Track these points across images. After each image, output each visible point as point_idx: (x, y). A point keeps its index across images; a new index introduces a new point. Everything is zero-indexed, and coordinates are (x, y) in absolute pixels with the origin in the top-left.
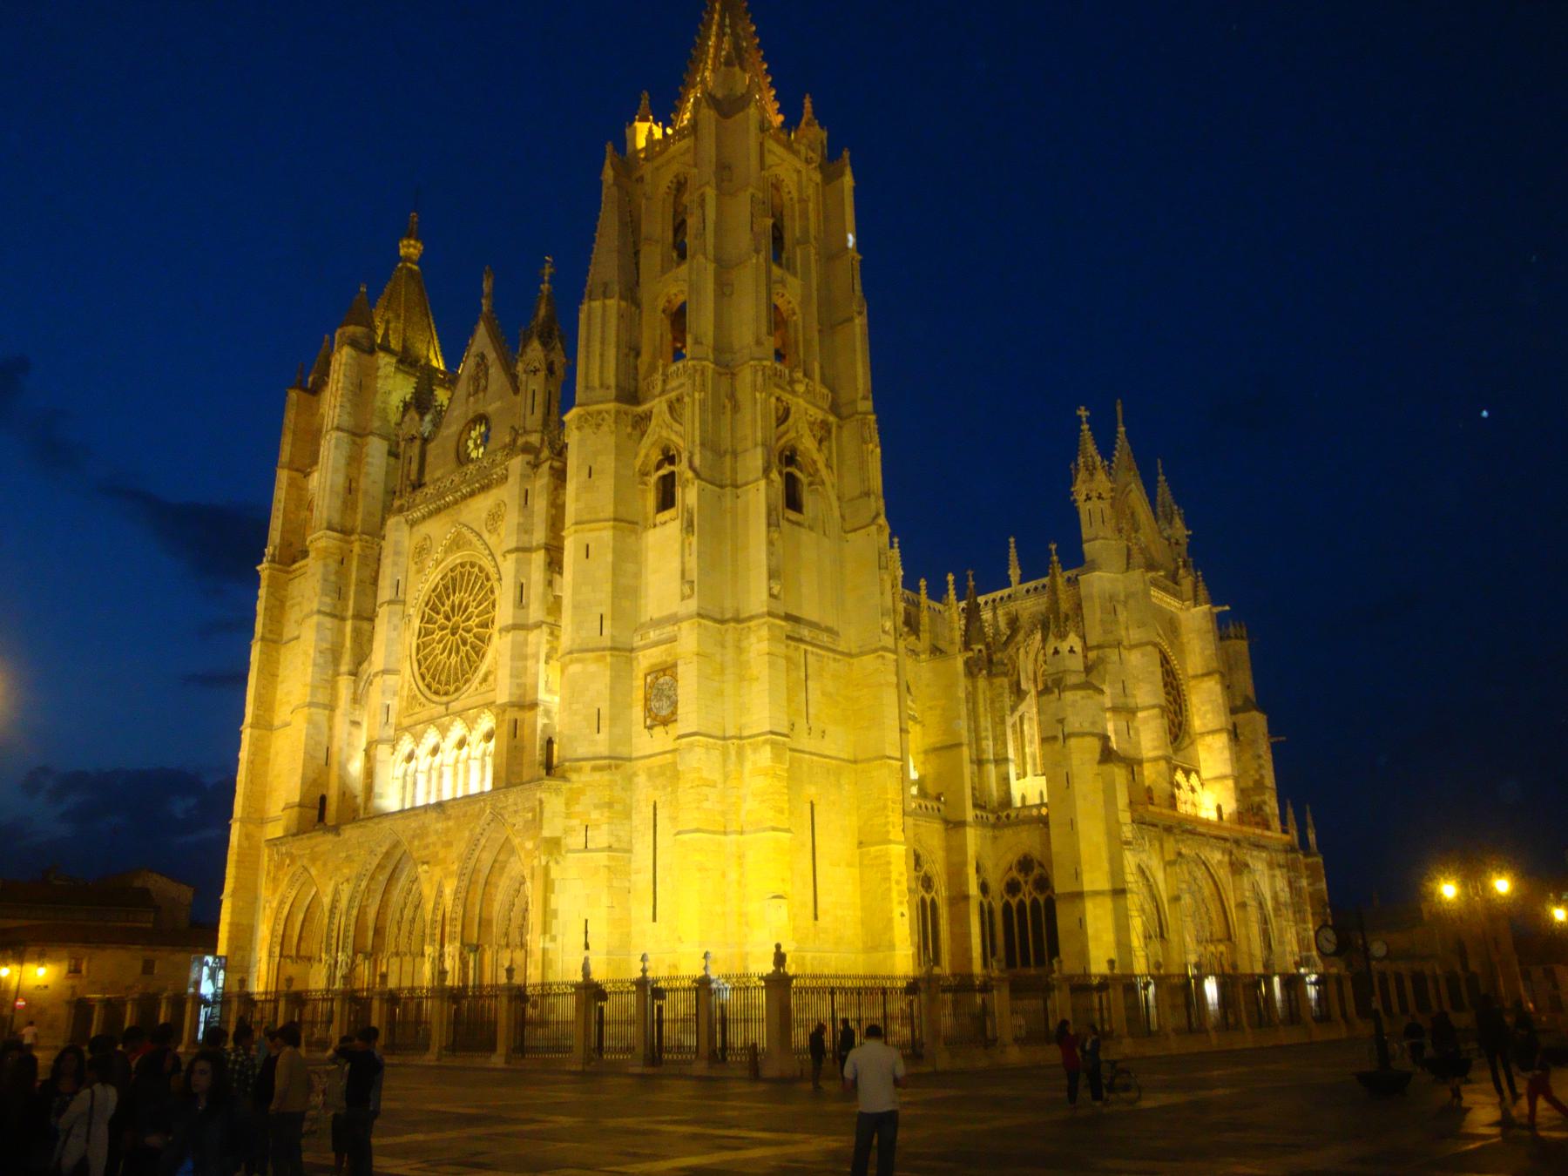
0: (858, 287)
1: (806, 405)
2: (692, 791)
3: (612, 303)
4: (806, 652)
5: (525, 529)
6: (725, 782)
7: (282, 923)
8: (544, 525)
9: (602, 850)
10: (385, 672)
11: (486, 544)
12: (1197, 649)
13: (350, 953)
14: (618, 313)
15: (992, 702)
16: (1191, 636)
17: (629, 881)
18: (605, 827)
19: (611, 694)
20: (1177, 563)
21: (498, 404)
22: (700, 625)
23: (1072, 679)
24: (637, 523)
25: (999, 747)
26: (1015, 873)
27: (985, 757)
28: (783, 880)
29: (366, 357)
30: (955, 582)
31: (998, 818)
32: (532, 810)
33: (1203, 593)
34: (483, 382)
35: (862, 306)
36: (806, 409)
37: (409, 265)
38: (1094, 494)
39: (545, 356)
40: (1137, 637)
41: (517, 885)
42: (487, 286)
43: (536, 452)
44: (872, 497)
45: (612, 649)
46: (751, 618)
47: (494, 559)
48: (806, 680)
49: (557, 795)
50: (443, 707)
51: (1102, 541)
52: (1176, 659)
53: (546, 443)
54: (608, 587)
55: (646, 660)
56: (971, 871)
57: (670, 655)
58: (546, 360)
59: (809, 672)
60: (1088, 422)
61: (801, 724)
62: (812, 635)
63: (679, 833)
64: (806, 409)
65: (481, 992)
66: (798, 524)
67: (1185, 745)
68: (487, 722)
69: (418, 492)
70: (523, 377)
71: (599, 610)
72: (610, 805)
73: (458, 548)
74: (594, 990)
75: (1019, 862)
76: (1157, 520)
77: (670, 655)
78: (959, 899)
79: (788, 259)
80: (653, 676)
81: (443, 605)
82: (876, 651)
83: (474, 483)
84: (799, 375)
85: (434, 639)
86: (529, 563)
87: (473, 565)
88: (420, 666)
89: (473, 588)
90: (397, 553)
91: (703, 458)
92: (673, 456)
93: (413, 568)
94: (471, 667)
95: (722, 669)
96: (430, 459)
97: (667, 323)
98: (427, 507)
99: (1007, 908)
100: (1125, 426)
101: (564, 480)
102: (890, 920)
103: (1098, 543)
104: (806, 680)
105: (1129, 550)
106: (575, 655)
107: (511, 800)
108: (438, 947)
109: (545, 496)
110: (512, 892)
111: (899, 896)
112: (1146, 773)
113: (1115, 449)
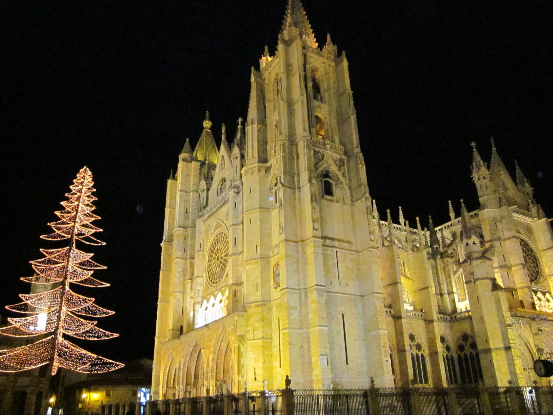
0: (352, 103)
1: (332, 153)
3: (255, 126)
4: (336, 252)
6: (301, 307)
10: (197, 277)
12: (543, 238)
13: (185, 385)
14: (257, 129)
15: (444, 269)
17: (272, 351)
18: (261, 329)
20: (528, 202)
21: (228, 172)
22: (286, 244)
23: (475, 255)
25: (449, 288)
26: (461, 342)
29: (189, 164)
30: (420, 220)
31: (452, 318)
33: (542, 213)
35: (354, 111)
37: (207, 130)
38: (481, 177)
42: (223, 130)
44: (363, 186)
45: (261, 258)
46: (307, 239)
51: (487, 196)
52: (534, 245)
55: (273, 262)
64: (332, 155)
66: (332, 201)
67: (541, 281)
69: (205, 209)
72: (262, 320)
75: (462, 336)
76: (516, 185)
80: (276, 267)
81: (214, 249)
82: (368, 249)
90: (200, 233)
91: (285, 178)
100: (496, 147)
103: (485, 197)
105: (500, 198)
106: (248, 262)
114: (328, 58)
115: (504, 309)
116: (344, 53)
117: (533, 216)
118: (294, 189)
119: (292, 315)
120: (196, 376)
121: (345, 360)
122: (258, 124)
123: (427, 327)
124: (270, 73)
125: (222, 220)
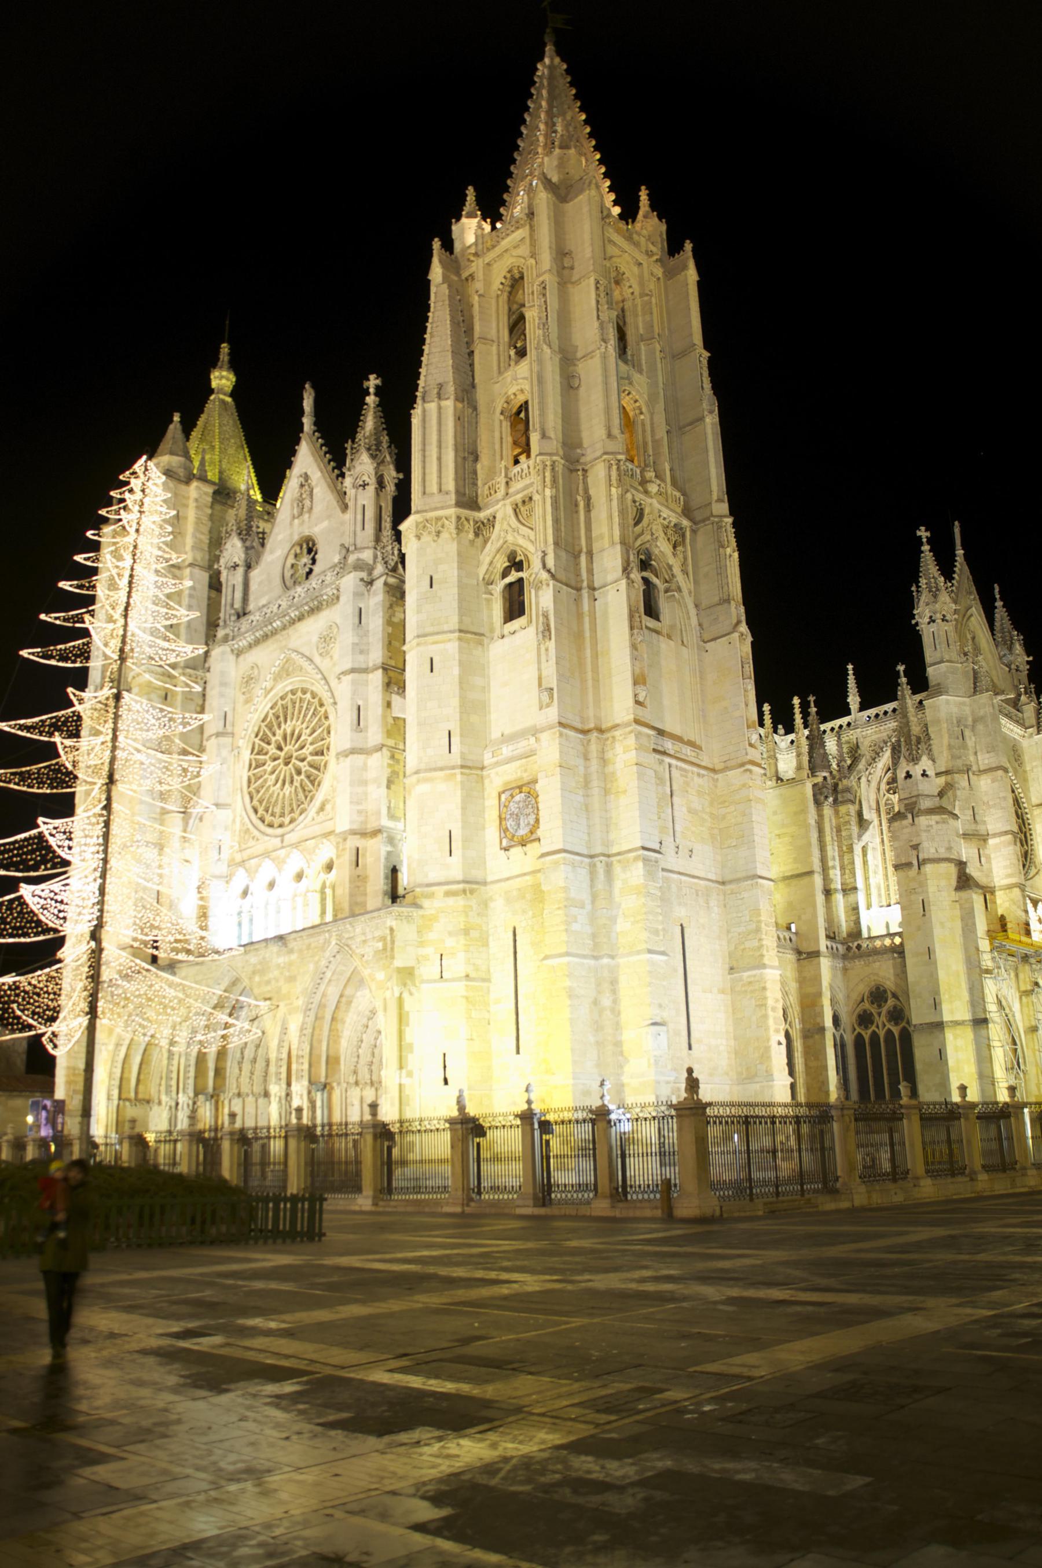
0: (707, 385)
1: (660, 507)
2: (560, 912)
3: (449, 404)
4: (670, 766)
5: (361, 649)
6: (593, 902)
7: (120, 1066)
8: (380, 645)
9: (459, 979)
11: (317, 667)
13: (192, 1094)
15: (839, 831)
16: (1034, 764)
19: (464, 814)
21: (325, 524)
22: (561, 735)
23: (925, 804)
24: (483, 635)
25: (847, 877)
26: (866, 1005)
27: (833, 886)
28: (660, 1006)
29: (183, 487)
31: (849, 949)
32: (383, 939)
34: (307, 503)
36: (660, 511)
37: (222, 396)
38: (939, 616)
39: (377, 469)
40: (986, 762)
41: (365, 1021)
42: (308, 403)
43: (370, 570)
45: (462, 767)
46: (616, 727)
47: (327, 683)
48: (671, 796)
49: (408, 922)
50: (279, 839)
53: (380, 558)
54: (455, 702)
55: (497, 779)
56: (826, 1002)
57: (526, 771)
58: (376, 473)
59: (674, 788)
60: (928, 542)
61: (668, 841)
62: (676, 748)
63: (546, 958)
65: (332, 1132)
68: (327, 851)
69: (243, 620)
70: (351, 492)
71: (446, 727)
72: (466, 932)
73: (288, 675)
74: (471, 1125)
75: (871, 993)
77: (526, 771)
78: (813, 1032)
79: (632, 355)
80: (508, 793)
81: (274, 734)
82: (742, 765)
83: (302, 606)
84: (650, 474)
85: (265, 771)
86: (366, 683)
87: (304, 692)
88: (252, 798)
89: (305, 716)
90: (224, 684)
91: (557, 557)
92: (521, 562)
93: (241, 698)
94: (306, 797)
95: (587, 784)
96: (253, 587)
97: (506, 425)
98: (253, 634)
99: (859, 1041)
101: (402, 595)
102: (768, 1049)
104: (671, 796)
106: (422, 775)
107: (358, 930)
108: (284, 1086)
109: (381, 614)
110: (360, 1028)
111: (776, 1023)
112: (999, 901)
113: (954, 572)
114: (649, 254)
115: (979, 935)
116: (688, 246)
117: (1027, 724)
118: (579, 589)
119: (576, 922)
120: (219, 1072)
121: (686, 1038)
122: (457, 399)
123: (800, 971)
124: (488, 264)
125: (303, 655)
